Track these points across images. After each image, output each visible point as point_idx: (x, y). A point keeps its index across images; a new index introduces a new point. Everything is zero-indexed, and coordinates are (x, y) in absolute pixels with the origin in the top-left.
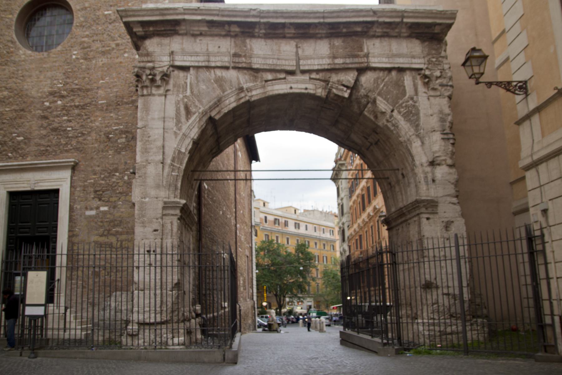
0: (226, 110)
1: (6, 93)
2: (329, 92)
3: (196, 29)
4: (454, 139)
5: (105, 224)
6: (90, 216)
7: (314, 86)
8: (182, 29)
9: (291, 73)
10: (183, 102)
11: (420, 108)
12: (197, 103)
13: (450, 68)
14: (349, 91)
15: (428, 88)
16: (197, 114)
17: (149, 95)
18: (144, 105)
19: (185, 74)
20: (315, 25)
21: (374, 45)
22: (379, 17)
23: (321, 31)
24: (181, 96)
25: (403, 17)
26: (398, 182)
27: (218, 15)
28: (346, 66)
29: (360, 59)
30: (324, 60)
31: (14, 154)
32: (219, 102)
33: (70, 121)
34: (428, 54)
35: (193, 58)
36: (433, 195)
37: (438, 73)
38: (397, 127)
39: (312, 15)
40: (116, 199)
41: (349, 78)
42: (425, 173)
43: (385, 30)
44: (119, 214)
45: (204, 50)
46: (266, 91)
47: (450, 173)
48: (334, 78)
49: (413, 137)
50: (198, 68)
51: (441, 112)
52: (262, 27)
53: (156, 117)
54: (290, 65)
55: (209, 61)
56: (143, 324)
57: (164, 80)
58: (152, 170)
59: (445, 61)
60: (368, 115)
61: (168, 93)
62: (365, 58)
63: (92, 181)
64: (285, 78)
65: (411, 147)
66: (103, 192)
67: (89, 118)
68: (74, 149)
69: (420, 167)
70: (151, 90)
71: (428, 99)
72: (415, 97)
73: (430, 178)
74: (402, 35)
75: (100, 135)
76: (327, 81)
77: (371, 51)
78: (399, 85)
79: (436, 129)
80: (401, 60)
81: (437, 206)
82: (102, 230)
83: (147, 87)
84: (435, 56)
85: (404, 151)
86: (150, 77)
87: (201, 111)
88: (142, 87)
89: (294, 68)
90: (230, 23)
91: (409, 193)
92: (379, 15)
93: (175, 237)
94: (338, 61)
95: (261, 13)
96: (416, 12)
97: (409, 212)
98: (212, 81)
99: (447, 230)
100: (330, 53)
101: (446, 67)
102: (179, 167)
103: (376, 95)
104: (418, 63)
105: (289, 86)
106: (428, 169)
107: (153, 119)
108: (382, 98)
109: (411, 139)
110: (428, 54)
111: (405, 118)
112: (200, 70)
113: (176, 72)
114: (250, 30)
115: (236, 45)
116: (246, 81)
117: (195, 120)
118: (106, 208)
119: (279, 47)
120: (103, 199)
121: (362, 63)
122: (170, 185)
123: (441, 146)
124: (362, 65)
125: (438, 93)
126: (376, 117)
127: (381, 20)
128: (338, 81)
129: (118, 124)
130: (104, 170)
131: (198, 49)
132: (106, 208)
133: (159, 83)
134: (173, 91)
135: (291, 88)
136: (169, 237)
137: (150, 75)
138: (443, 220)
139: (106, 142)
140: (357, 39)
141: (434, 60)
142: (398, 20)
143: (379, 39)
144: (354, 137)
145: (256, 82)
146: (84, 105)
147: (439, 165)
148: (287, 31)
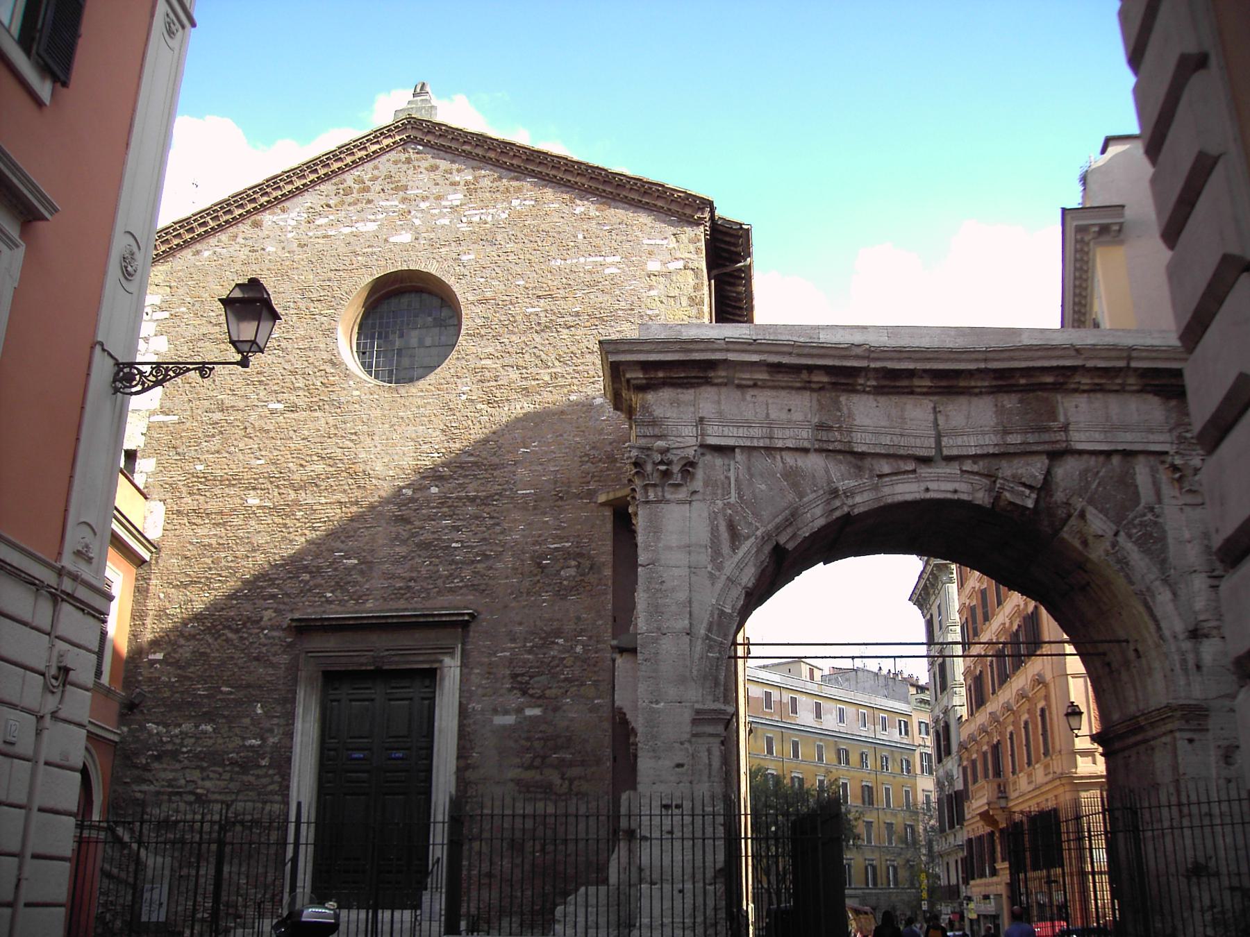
0: (806, 532)
1: (320, 467)
2: (997, 498)
3: (747, 376)
6: (504, 727)
7: (970, 486)
9: (925, 461)
10: (725, 515)
11: (1167, 528)
14: (1034, 496)
16: (752, 539)
19: (726, 462)
20: (970, 374)
21: (1077, 407)
22: (1087, 359)
23: (979, 384)
25: (1129, 359)
26: (1126, 663)
27: (790, 354)
29: (1052, 435)
30: (987, 436)
31: (338, 593)
32: (793, 517)
33: (457, 529)
35: (741, 432)
38: (1127, 564)
39: (964, 356)
41: (1034, 469)
42: (1183, 654)
43: (1097, 381)
48: (1007, 469)
49: (1157, 583)
53: (674, 543)
54: (925, 446)
58: (669, 647)
60: (1070, 540)
61: (695, 497)
64: (914, 471)
67: (498, 524)
68: (466, 586)
70: (663, 491)
71: (1181, 509)
76: (991, 476)
77: (1071, 419)
78: (1126, 482)
80: (1129, 437)
83: (655, 485)
86: (663, 468)
87: (759, 533)
88: (646, 487)
89: (932, 453)
90: (811, 369)
93: (716, 779)
94: (1011, 439)
95: (871, 352)
100: (997, 424)
103: (1084, 503)
104: (1160, 441)
105: (923, 486)
106: (1187, 645)
110: (1178, 425)
111: (1140, 546)
112: (755, 454)
113: (708, 457)
115: (821, 407)
116: (842, 475)
117: (748, 551)
119: (903, 410)
121: (1057, 442)
122: (705, 678)
126: (1085, 543)
127: (1090, 364)
128: (1014, 476)
129: (561, 539)
131: (749, 415)
133: (678, 479)
135: (927, 490)
136: (705, 778)
137: (662, 462)
138: (1220, 743)
139: (536, 575)
140: (1045, 395)
142: (1122, 364)
143: (1086, 395)
147: (1207, 636)
148: (917, 382)
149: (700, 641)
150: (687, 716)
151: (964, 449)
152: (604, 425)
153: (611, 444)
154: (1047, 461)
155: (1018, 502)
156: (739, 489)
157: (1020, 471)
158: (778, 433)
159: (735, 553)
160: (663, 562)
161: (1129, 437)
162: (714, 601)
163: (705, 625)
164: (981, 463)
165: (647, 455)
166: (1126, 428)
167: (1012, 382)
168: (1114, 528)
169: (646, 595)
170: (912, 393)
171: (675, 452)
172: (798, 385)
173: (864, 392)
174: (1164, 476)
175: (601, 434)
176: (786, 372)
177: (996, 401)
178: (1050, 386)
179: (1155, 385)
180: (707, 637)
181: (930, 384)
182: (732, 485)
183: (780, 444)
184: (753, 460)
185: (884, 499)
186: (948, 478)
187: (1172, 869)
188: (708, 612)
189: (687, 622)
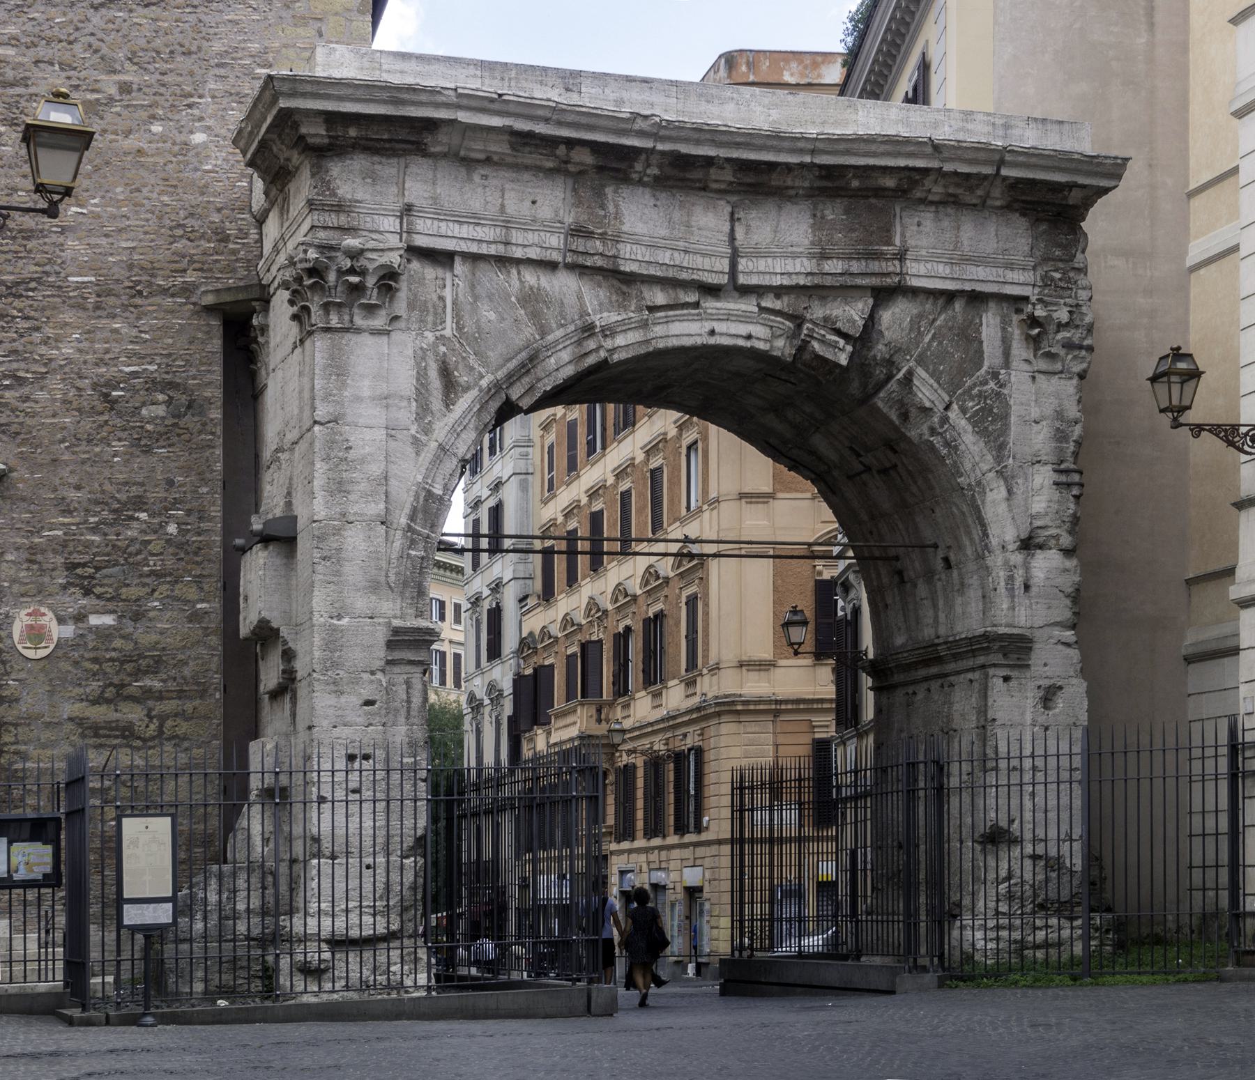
2: (803, 347)
4: (1082, 485)
5: (107, 667)
7: (768, 330)
9: (712, 291)
11: (1012, 403)
12: (472, 360)
13: (1090, 299)
14: (849, 348)
15: (1036, 349)
16: (474, 393)
17: (346, 330)
19: (440, 272)
21: (919, 225)
24: (430, 336)
28: (849, 281)
29: (884, 264)
34: (1045, 259)
35: (465, 231)
36: (1022, 623)
37: (1063, 315)
38: (956, 448)
40: (143, 591)
41: (853, 313)
42: (1011, 568)
43: (951, 191)
44: (154, 637)
45: (493, 210)
46: (652, 335)
47: (1066, 570)
49: (992, 475)
50: (474, 258)
51: (1059, 414)
52: (654, 160)
53: (366, 393)
54: (714, 269)
55: (507, 244)
56: (339, 943)
57: (390, 288)
58: (356, 542)
59: (1083, 282)
60: (885, 410)
61: (397, 325)
62: (897, 262)
63: (60, 533)
64: (696, 305)
65: (983, 502)
66: (98, 569)
70: (352, 316)
71: (1034, 378)
72: (1003, 371)
73: (1019, 581)
74: (989, 202)
75: (79, 389)
77: (911, 242)
79: (1044, 458)
80: (981, 272)
81: (1030, 649)
82: (95, 686)
83: (340, 305)
84: (1061, 265)
85: (965, 508)
86: (354, 279)
87: (484, 383)
88: (326, 307)
89: (724, 280)
90: (570, 143)
92: (946, 154)
93: (416, 721)
96: (1034, 155)
98: (513, 299)
99: (1046, 707)
100: (812, 243)
102: (428, 537)
104: (1020, 282)
105: (708, 326)
106: (1017, 558)
107: (358, 399)
108: (927, 371)
109: (984, 482)
110: (1045, 259)
111: (974, 425)
112: (483, 266)
113: (415, 265)
116: (601, 304)
117: (470, 408)
118: (109, 620)
120: (98, 590)
121: (888, 275)
122: (405, 584)
123: (1050, 501)
125: (1059, 366)
126: (905, 416)
127: (948, 167)
128: (826, 319)
130: (97, 503)
132: (109, 620)
134: (408, 320)
136: (402, 720)
137: (352, 271)
141: (1057, 275)
142: (988, 170)
143: (933, 209)
145: (625, 308)
146: (18, 284)
147: (1041, 547)
149: (399, 533)
150: (381, 636)
151: (767, 277)
155: (829, 356)
156: (458, 317)
158: (517, 237)
159: (449, 410)
160: (349, 419)
162: (420, 478)
163: (407, 510)
164: (786, 299)
165: (329, 258)
168: (947, 399)
170: (704, 189)
171: (370, 255)
172: (550, 164)
173: (640, 183)
174: (1016, 333)
176: (536, 145)
177: (815, 208)
178: (890, 193)
179: (1023, 202)
181: (732, 179)
182: (449, 309)
183: (518, 253)
184: (478, 274)
185: (653, 342)
186: (744, 318)
187: (966, 831)
188: (412, 493)
189: (382, 506)
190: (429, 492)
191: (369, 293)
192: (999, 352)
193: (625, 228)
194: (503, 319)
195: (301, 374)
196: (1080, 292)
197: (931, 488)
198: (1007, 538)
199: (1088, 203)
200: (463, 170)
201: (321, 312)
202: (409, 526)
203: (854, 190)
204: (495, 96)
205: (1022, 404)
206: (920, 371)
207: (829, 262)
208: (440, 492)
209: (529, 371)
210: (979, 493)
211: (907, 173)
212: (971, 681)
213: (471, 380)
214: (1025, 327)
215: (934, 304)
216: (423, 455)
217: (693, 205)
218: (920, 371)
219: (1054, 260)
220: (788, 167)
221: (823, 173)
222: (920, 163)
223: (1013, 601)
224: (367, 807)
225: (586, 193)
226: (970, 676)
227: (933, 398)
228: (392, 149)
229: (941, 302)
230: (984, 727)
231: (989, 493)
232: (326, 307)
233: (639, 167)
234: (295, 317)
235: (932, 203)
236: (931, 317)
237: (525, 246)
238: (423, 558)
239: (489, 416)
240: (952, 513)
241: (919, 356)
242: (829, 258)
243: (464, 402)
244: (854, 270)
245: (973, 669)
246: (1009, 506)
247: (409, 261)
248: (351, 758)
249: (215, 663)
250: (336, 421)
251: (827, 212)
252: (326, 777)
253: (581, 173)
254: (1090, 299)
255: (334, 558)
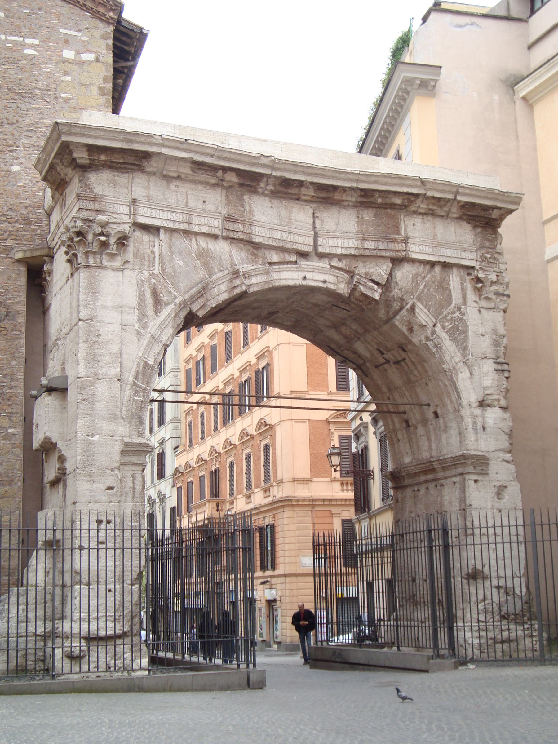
7: (335, 278)
8: (152, 166)
9: (303, 255)
11: (468, 324)
12: (170, 288)
13: (506, 269)
14: (380, 290)
15: (480, 296)
16: (172, 306)
17: (98, 267)
18: (90, 282)
19: (152, 238)
24: (146, 273)
25: (457, 193)
26: (425, 422)
27: (212, 156)
29: (397, 245)
30: (350, 241)
34: (481, 247)
35: (166, 215)
36: (483, 449)
37: (493, 277)
38: (441, 348)
39: (343, 176)
43: (431, 207)
46: (271, 278)
47: (505, 419)
48: (361, 269)
49: (461, 364)
50: (172, 231)
51: (495, 332)
52: (271, 181)
53: (110, 304)
55: (189, 223)
57: (124, 244)
61: (127, 266)
62: (403, 244)
64: (296, 263)
65: (457, 379)
69: (467, 407)
70: (101, 260)
71: (480, 311)
72: (463, 307)
73: (479, 426)
74: (450, 215)
76: (351, 273)
77: (410, 234)
79: (488, 355)
80: (448, 252)
81: (488, 464)
83: (94, 253)
84: (490, 250)
85: (447, 383)
86: (103, 239)
87: (177, 301)
88: (87, 254)
89: (310, 249)
90: (225, 169)
91: (444, 441)
92: (428, 186)
95: (275, 164)
96: (474, 189)
97: (444, 469)
98: (193, 255)
101: (503, 267)
103: (415, 300)
105: (302, 275)
106: (478, 411)
107: (106, 307)
108: (422, 304)
109: (457, 368)
110: (481, 247)
112: (175, 235)
113: (138, 233)
114: (253, 184)
115: (229, 203)
116: (242, 260)
117: (169, 315)
119: (290, 213)
121: (399, 251)
122: (132, 417)
123: (493, 380)
124: (400, 254)
125: (492, 305)
126: (411, 330)
127: (429, 194)
128: (366, 274)
133: (113, 249)
134: (133, 264)
135: (305, 278)
137: (102, 234)
141: (488, 256)
142: (451, 196)
143: (421, 217)
144: (359, 347)
145: (256, 263)
147: (489, 406)
148: (303, 190)
149: (128, 387)
150: (118, 447)
151: (334, 249)
152: (20, 190)
153: (26, 208)
154: (390, 265)
155: (369, 294)
156: (162, 264)
157: (371, 271)
158: (195, 220)
159: (158, 316)
160: (99, 318)
161: (448, 252)
162: (140, 354)
163: (133, 373)
164: (344, 261)
165: (89, 226)
166: (446, 245)
167: (372, 200)
168: (434, 321)
169: (86, 346)
170: (298, 199)
171: (111, 226)
172: (213, 181)
173: (263, 194)
174: (469, 286)
175: (17, 198)
176: (206, 170)
177: (358, 213)
178: (398, 207)
179: (469, 215)
180: (134, 384)
181: (314, 194)
183: (196, 229)
184: (173, 240)
186: (321, 271)
188: (136, 363)
189: (118, 370)
190: (146, 362)
191: (111, 247)
192: (460, 296)
193: (254, 218)
194: (188, 265)
195: (71, 293)
196: (500, 265)
197: (426, 371)
198: (471, 400)
199: (502, 218)
200: (165, 182)
201: (84, 257)
202: (134, 382)
203: (379, 204)
204: (184, 141)
205: (474, 325)
206: (419, 304)
207: (367, 242)
208: (153, 363)
209: (202, 295)
210: (455, 374)
211: (408, 196)
212: (454, 483)
213: (170, 299)
214: (473, 283)
215: (424, 268)
216: (142, 341)
217: (292, 208)
218: (419, 304)
219: (485, 247)
220: (344, 189)
221: (363, 194)
222: (414, 191)
223: (477, 436)
224: (111, 552)
225: (233, 198)
226: (454, 479)
227: (427, 320)
228: (125, 168)
229: (428, 267)
230: (464, 510)
231: (460, 374)
232: (87, 254)
233: (262, 185)
234: (69, 261)
235: (420, 214)
236: (423, 275)
237: (200, 225)
238: (142, 402)
239: (180, 320)
240: (439, 386)
241: (418, 296)
242: (367, 240)
243: (167, 311)
244: (381, 247)
245: (455, 476)
246: (471, 382)
247: (134, 231)
248: (99, 522)
249: (19, 464)
250: (91, 319)
251: (364, 216)
252: (85, 534)
253: (231, 187)
254: (506, 269)
255: (90, 400)
